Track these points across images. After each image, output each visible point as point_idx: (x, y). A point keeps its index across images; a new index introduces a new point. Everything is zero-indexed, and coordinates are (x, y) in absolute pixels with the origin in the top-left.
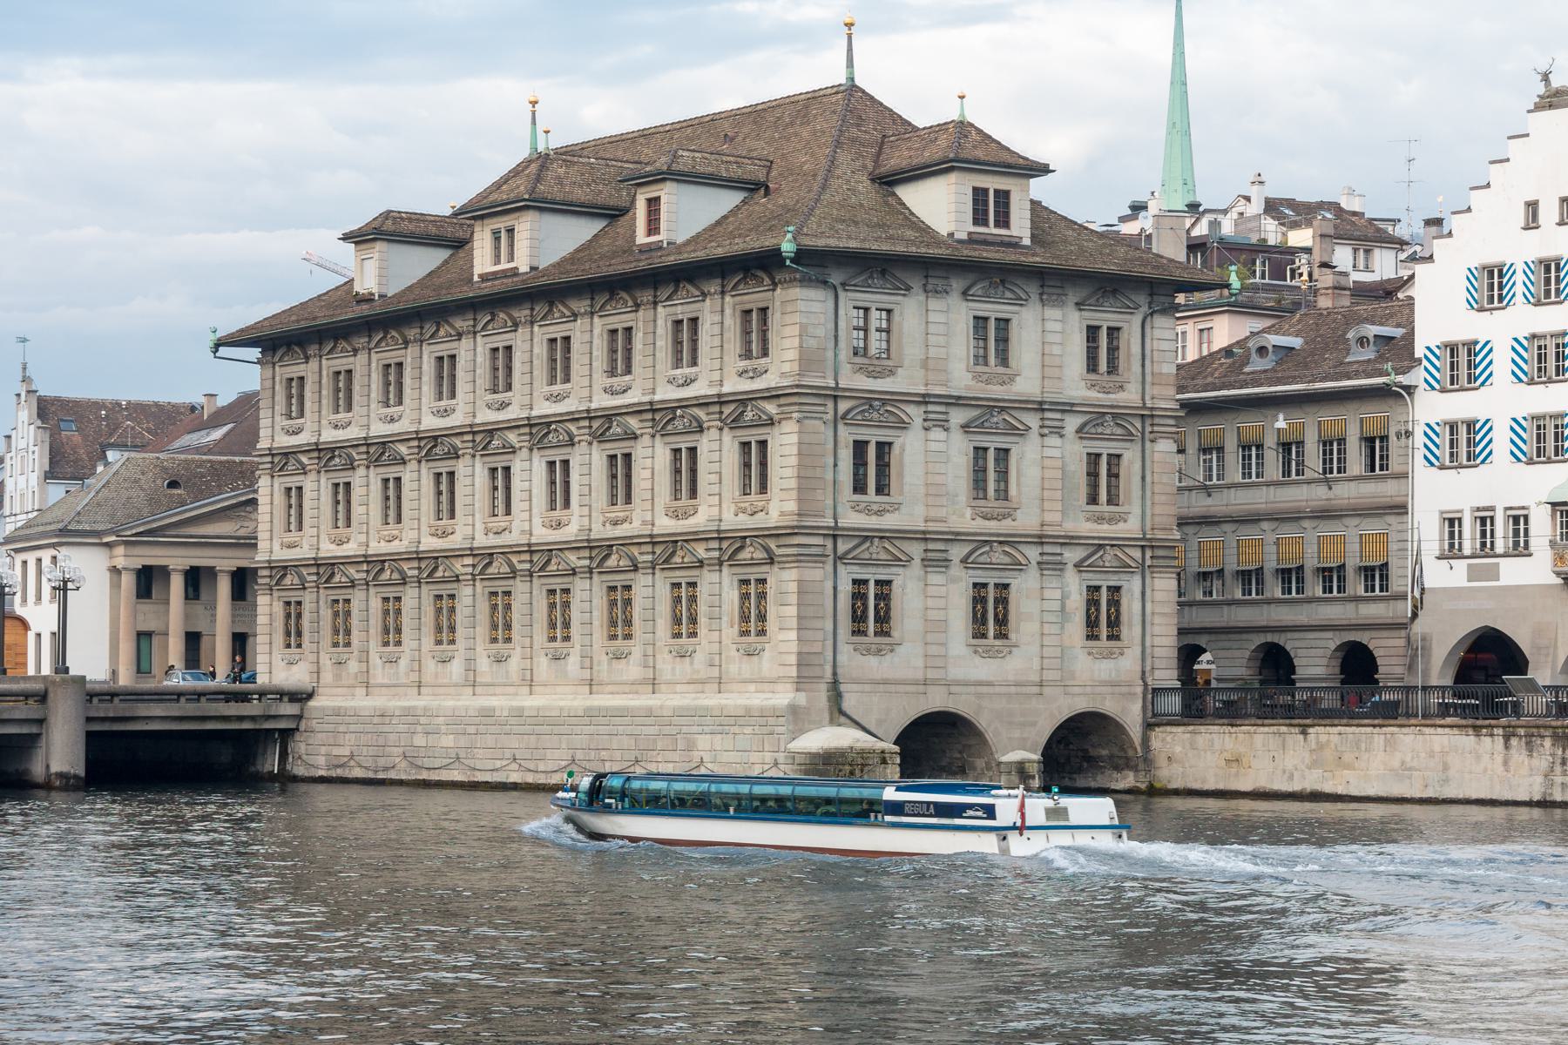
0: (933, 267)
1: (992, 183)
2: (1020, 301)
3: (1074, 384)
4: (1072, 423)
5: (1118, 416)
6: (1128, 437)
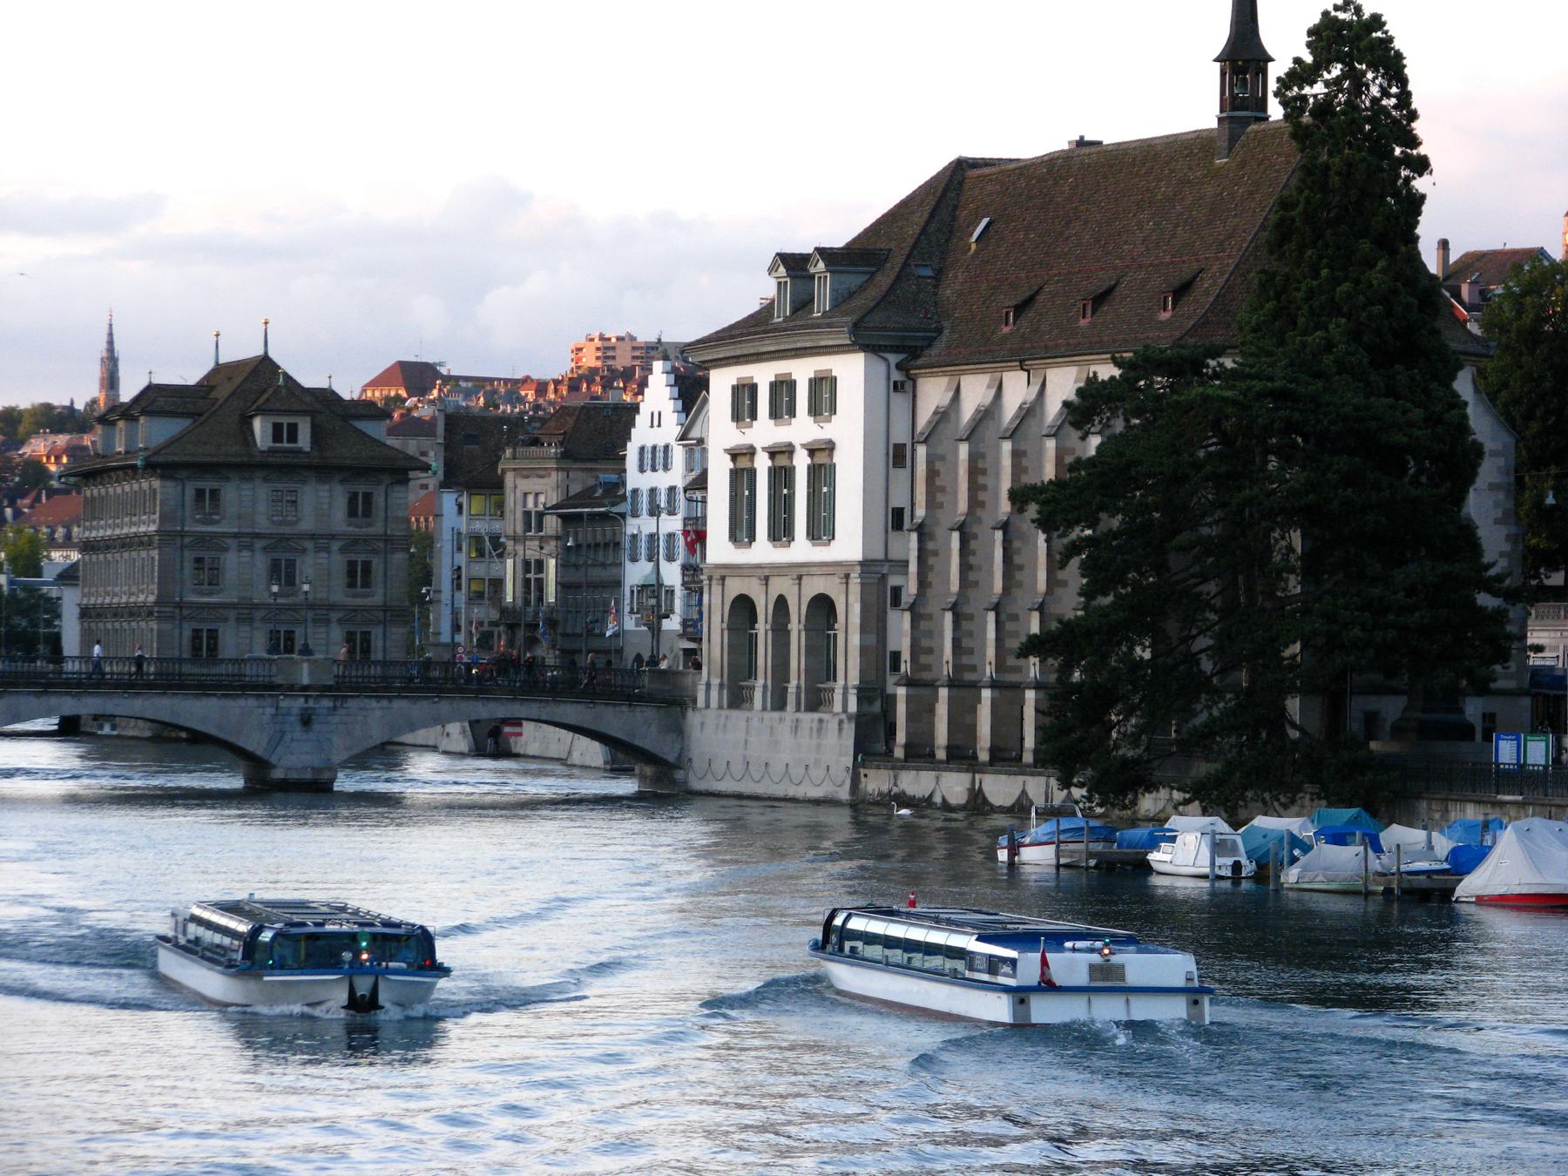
0: (250, 466)
1: (285, 420)
2: (304, 482)
3: (338, 519)
4: (336, 546)
5: (366, 540)
6: (375, 551)
